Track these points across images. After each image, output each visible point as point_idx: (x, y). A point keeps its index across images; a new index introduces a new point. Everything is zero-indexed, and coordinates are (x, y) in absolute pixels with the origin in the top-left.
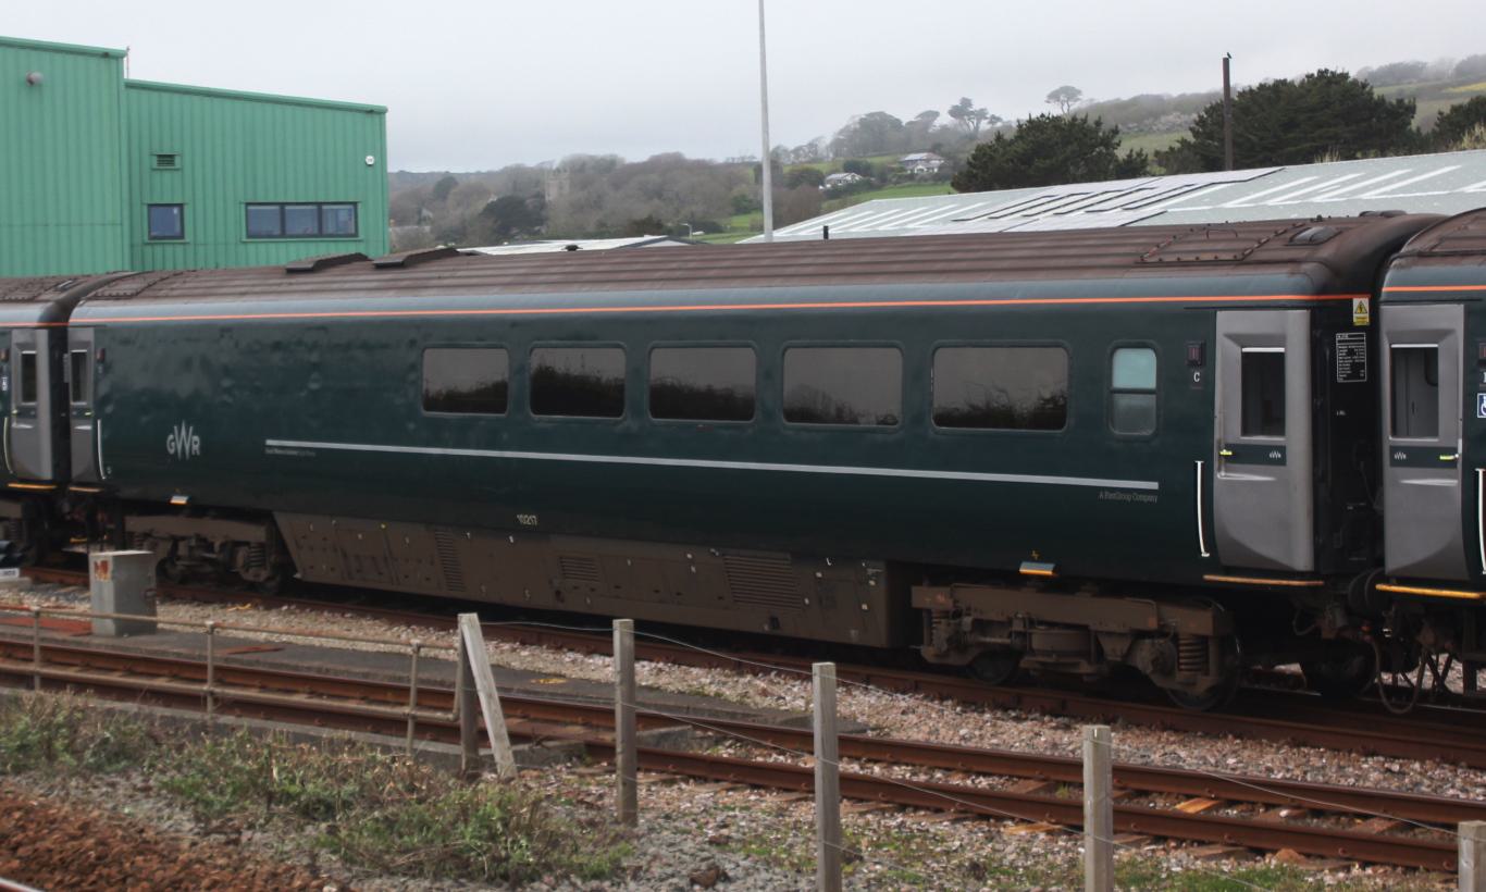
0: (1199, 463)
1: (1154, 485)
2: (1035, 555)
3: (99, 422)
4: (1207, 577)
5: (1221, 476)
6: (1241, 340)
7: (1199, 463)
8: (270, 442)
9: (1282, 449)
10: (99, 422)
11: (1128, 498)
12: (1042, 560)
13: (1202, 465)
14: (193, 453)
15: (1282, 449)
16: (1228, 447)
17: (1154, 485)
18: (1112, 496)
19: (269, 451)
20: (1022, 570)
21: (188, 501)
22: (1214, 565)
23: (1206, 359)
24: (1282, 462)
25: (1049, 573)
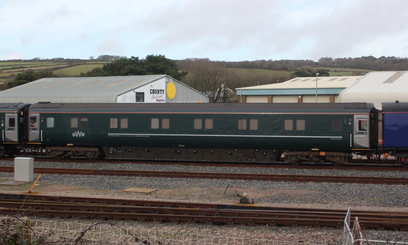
0: (351, 135)
1: (342, 137)
2: (315, 148)
3: (42, 131)
4: (353, 149)
5: (355, 136)
6: (358, 118)
7: (351, 135)
8: (109, 134)
9: (366, 132)
10: (42, 131)
11: (336, 139)
12: (317, 148)
13: (352, 135)
14: (82, 136)
15: (366, 132)
16: (356, 132)
17: (342, 137)
18: (333, 139)
19: (108, 136)
20: (312, 150)
21: (73, 144)
22: (353, 147)
23: (352, 122)
24: (366, 134)
25: (318, 150)
